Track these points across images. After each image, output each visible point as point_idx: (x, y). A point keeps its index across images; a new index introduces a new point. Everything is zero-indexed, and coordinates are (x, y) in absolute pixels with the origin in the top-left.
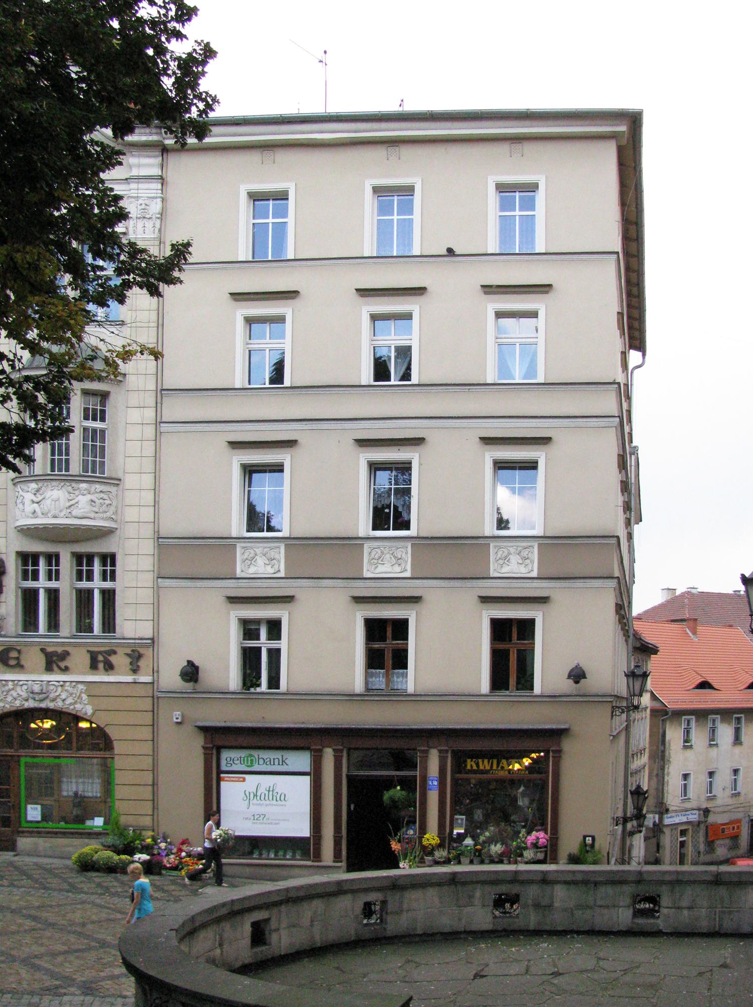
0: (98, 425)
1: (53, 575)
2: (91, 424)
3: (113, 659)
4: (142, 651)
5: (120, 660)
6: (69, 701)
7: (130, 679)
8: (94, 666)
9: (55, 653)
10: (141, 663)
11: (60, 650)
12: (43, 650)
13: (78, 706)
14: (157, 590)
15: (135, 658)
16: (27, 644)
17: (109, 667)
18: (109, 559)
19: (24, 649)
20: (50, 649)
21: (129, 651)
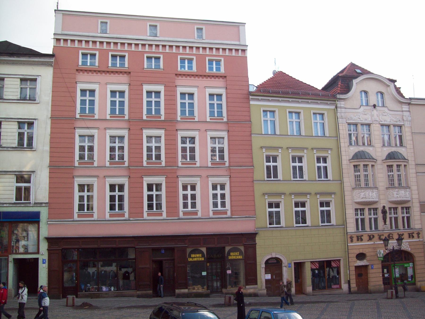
0: (356, 174)
1: (396, 213)
2: (358, 173)
3: (414, 235)
4: (420, 232)
5: (415, 235)
6: (405, 247)
7: (418, 240)
8: (409, 237)
9: (401, 234)
10: (420, 235)
11: (402, 233)
12: (398, 234)
13: (407, 248)
14: (421, 215)
15: (418, 234)
16: (394, 232)
17: (413, 237)
18: (408, 208)
19: (394, 234)
20: (399, 233)
21: (417, 232)
